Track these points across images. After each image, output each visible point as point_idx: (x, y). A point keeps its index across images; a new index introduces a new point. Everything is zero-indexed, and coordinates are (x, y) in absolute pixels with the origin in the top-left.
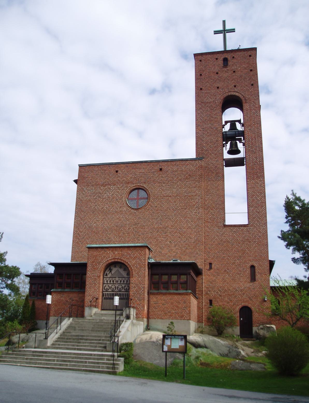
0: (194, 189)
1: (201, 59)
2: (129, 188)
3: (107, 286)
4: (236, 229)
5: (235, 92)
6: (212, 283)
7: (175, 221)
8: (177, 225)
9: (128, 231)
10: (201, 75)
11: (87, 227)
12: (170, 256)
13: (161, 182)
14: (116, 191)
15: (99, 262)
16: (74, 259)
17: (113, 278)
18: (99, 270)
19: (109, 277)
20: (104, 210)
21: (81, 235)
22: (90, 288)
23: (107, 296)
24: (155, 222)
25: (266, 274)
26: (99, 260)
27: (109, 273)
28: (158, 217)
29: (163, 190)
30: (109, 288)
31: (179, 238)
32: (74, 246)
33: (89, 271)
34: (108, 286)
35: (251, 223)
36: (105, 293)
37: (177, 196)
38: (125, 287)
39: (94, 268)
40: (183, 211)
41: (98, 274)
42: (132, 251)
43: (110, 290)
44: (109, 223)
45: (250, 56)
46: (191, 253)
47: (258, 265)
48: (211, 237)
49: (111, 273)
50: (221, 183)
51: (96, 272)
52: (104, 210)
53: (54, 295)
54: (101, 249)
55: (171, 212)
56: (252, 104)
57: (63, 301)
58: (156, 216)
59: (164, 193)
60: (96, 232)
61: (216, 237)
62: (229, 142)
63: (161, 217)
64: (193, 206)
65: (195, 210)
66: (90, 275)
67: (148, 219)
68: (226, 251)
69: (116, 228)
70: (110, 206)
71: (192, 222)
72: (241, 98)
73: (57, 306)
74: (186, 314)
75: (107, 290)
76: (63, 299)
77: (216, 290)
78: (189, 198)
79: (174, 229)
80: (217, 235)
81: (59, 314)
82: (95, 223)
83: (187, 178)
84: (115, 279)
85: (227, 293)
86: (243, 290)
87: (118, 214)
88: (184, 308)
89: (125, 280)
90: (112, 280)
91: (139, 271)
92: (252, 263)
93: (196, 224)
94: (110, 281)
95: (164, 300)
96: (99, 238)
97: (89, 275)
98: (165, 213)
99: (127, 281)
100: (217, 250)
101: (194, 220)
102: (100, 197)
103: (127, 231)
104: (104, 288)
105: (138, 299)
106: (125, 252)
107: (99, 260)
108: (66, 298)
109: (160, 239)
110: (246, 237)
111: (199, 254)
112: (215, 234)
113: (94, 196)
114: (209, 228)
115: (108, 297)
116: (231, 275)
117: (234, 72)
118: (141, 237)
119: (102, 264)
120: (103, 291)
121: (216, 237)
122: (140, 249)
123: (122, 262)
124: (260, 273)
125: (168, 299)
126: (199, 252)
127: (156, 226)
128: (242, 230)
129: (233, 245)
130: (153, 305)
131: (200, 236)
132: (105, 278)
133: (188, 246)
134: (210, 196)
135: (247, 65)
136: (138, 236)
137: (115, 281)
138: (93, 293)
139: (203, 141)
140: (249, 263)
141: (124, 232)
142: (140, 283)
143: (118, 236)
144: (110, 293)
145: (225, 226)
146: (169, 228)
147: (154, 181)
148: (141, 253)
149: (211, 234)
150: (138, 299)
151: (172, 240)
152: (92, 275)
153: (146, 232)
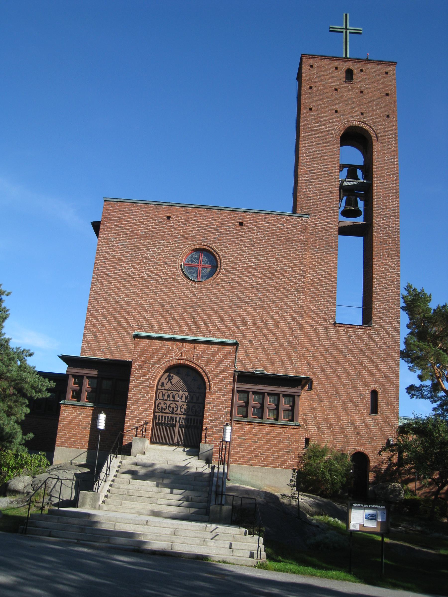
0: (292, 262)
1: (312, 64)
2: (188, 246)
3: (162, 404)
4: (353, 331)
5: (362, 122)
6: (311, 412)
7: (259, 308)
8: (262, 315)
9: (181, 315)
10: (311, 88)
11: (112, 301)
12: (248, 363)
13: (240, 244)
14: (166, 249)
15: (153, 361)
16: (86, 352)
17: (174, 391)
18: (153, 376)
19: (167, 389)
20: (143, 276)
21: (102, 313)
23: (162, 421)
24: (227, 307)
25: (393, 405)
26: (153, 359)
27: (167, 382)
28: (233, 298)
29: (243, 257)
31: (264, 336)
32: (87, 330)
33: (135, 376)
34: (164, 404)
35: (376, 326)
37: (265, 268)
39: (144, 372)
40: (273, 293)
42: (211, 349)
43: (167, 411)
44: (149, 300)
45: (386, 73)
46: (282, 362)
47: (382, 391)
48: (314, 340)
49: (171, 383)
50: (334, 257)
51: (147, 379)
52: (143, 276)
53: (65, 410)
54: (157, 341)
55: (255, 293)
56: (387, 144)
58: (230, 296)
59: (244, 261)
61: (322, 341)
62: (345, 198)
63: (238, 299)
64: (290, 288)
65: (292, 295)
67: (216, 301)
68: (335, 365)
69: (162, 308)
70: (155, 272)
71: (286, 312)
72: (371, 134)
74: (290, 459)
75: (162, 410)
76: (81, 419)
77: (317, 423)
78: (283, 275)
79: (257, 320)
80: (324, 338)
81: (72, 443)
82: (126, 296)
83: (282, 243)
85: (333, 429)
86: (359, 427)
87: (166, 287)
88: (287, 449)
91: (222, 383)
92: (375, 386)
93: (292, 316)
94: (168, 396)
95: (256, 435)
96: (131, 322)
98: (243, 294)
100: (321, 362)
101: (291, 311)
102: (137, 255)
103: (179, 315)
104: (158, 406)
105: (217, 430)
106: (200, 351)
107: (153, 359)
108: (87, 417)
109: (233, 335)
110: (368, 345)
111: (295, 365)
112: (320, 335)
113: (127, 252)
114: (312, 325)
115: (163, 422)
116: (340, 401)
117: (362, 92)
118: (202, 328)
120: (155, 412)
121: (322, 341)
123: (194, 365)
124: (385, 403)
125: (262, 433)
126: (294, 361)
127: (229, 312)
128: (361, 333)
129: (347, 356)
130: (237, 440)
131: (299, 337)
132: (159, 389)
133: (279, 350)
134: (316, 275)
135: (381, 86)
136: (197, 326)
137: (177, 395)
138: (141, 413)
139: (309, 188)
140: (370, 386)
141: (175, 316)
143: (164, 323)
144: (167, 415)
145: (337, 325)
146: (249, 318)
147: (229, 240)
149: (314, 335)
150: (217, 430)
151: (254, 339)
152: (140, 383)
153: (211, 320)
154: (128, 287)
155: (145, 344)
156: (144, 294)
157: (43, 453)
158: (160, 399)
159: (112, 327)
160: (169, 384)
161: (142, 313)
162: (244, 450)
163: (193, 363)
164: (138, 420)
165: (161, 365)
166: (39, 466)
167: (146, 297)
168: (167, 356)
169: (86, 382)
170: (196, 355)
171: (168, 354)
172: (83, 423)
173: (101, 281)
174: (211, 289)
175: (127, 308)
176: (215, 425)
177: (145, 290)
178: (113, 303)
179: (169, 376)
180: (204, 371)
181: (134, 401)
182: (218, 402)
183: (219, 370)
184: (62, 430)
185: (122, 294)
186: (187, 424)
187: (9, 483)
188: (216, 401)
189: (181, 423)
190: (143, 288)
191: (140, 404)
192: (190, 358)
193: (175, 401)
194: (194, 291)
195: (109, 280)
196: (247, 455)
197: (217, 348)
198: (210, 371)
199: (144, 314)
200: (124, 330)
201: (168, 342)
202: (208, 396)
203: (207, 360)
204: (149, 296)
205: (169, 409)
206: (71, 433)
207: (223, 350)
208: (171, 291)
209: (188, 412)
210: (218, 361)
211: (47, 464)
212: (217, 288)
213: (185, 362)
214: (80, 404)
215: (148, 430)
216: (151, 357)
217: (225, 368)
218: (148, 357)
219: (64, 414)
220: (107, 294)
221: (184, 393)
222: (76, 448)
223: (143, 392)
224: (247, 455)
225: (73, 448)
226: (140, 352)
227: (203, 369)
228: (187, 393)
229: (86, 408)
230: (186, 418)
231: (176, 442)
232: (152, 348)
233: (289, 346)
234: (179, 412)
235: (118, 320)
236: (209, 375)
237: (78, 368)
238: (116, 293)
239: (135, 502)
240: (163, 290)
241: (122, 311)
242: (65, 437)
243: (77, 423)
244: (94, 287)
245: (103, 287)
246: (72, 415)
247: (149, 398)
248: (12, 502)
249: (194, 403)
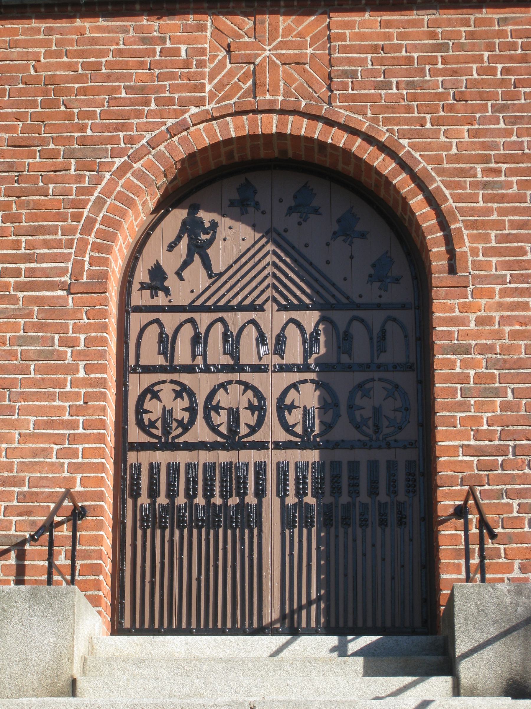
15: (82, 141)
19: (185, 302)
27: (186, 264)
34: (178, 395)
38: (358, 401)
39: (38, 206)
41: (78, 265)
42: (433, 35)
49: (207, 264)
51: (58, 244)
54: (101, 22)
75: (166, 431)
89: (357, 329)
90: (219, 328)
99: (383, 332)
104: (140, 411)
106: (363, 50)
115: (181, 500)
119: (118, 162)
132: (138, 309)
137: (251, 333)
138: (35, 453)
155: (26, 44)
158: (148, 369)
163: (330, 123)
164: (22, 497)
165: (136, 157)
168: (170, 101)
170: (345, 74)
171: (174, 89)
176: (512, 479)
180: (403, 165)
182: (514, 335)
183: (494, 147)
186: (328, 499)
188: (499, 335)
189: (291, 500)
191: (25, 396)
192: (311, 98)
193: (242, 369)
197: (466, 23)
198: (438, 160)
201: (166, 22)
203: (414, 97)
205: (208, 419)
207: (501, 34)
209: (327, 427)
210: (482, 96)
213: (282, 124)
215: (88, 555)
216: (70, 117)
218: (51, 116)
221: (296, 315)
223: (40, 327)
227: (392, 154)
228: (315, 315)
230: (320, 466)
231: (277, 615)
232: (69, 67)
247: (78, 356)
249: (365, 367)
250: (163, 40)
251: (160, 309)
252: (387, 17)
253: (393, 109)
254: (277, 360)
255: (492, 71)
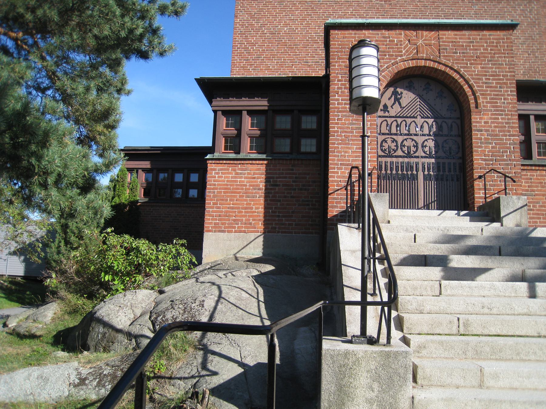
3: (389, 141)
17: (406, 117)
19: (394, 115)
22: (343, 142)
27: (394, 104)
30: (397, 146)
34: (393, 142)
36: (383, 160)
40: (493, 5)
42: (469, 39)
43: (399, 153)
44: (319, 26)
53: (215, 170)
54: (371, 32)
57: (246, 185)
58: (433, 13)
60: (291, 45)
66: (342, 104)
73: (227, 200)
76: (243, 182)
82: (286, 25)
84: (414, 121)
87: (341, 8)
89: (444, 125)
91: (497, 95)
96: (297, 58)
97: (338, 104)
98: (452, 9)
99: (452, 125)
104: (381, 146)
106: (449, 42)
108: (254, 178)
115: (394, 172)
122: (494, 35)
142: (504, 131)
144: (401, 160)
148: (497, 46)
154: (287, 13)
155: (349, 38)
156: (310, 19)
157: (181, 242)
158: (383, 134)
159: (270, 67)
160: (397, 108)
161: (311, 45)
162: (533, 214)
163: (440, 63)
166: (177, 268)
167: (314, 24)
168: (393, 55)
169: (247, 121)
171: (393, 52)
172: (249, 189)
173: (249, 9)
174: (405, 6)
175: (289, 40)
177: (311, 15)
178: (267, 36)
179: (395, 93)
180: (462, 76)
181: (341, 136)
182: (495, 127)
183: (488, 72)
184: (214, 204)
185: (279, 22)
187: (95, 313)
188: (491, 127)
189: (426, 173)
190: (309, 13)
191: (353, 140)
192: (434, 56)
193: (411, 135)
194: (381, 11)
195: (259, 7)
196: (540, 222)
197: (479, 35)
198: (472, 75)
199: (314, 46)
200: (287, 69)
201: (390, 32)
202: (475, 118)
203: (464, 57)
204: (317, 22)
205: (401, 149)
206: (228, 208)
207: (490, 39)
208: (349, 13)
210: (484, 57)
211: (191, 262)
212: (413, 4)
214: (239, 156)
217: (498, 68)
219: (215, 177)
220: (258, 25)
221: (426, 120)
222: (240, 232)
224: (540, 222)
225: (236, 232)
226: (341, 52)
228: (433, 120)
229: (250, 162)
233: (525, 75)
234: (420, 153)
235: (277, 57)
236: (472, 82)
237: (230, 99)
238: (270, 22)
239: (511, 360)
240: (337, 13)
241: (282, 45)
242: (220, 216)
243: (238, 189)
244: (240, 18)
245: (252, 17)
246: (228, 177)
248: (82, 381)
250: (389, 37)
251: (387, 117)
252: (456, 33)
253: (458, 60)
254: (421, 133)
255: (487, 50)
